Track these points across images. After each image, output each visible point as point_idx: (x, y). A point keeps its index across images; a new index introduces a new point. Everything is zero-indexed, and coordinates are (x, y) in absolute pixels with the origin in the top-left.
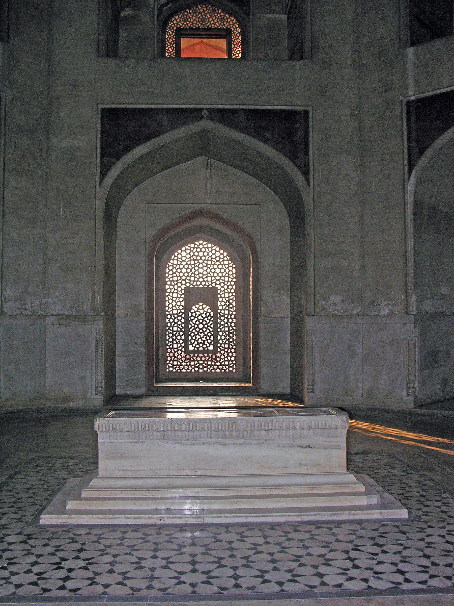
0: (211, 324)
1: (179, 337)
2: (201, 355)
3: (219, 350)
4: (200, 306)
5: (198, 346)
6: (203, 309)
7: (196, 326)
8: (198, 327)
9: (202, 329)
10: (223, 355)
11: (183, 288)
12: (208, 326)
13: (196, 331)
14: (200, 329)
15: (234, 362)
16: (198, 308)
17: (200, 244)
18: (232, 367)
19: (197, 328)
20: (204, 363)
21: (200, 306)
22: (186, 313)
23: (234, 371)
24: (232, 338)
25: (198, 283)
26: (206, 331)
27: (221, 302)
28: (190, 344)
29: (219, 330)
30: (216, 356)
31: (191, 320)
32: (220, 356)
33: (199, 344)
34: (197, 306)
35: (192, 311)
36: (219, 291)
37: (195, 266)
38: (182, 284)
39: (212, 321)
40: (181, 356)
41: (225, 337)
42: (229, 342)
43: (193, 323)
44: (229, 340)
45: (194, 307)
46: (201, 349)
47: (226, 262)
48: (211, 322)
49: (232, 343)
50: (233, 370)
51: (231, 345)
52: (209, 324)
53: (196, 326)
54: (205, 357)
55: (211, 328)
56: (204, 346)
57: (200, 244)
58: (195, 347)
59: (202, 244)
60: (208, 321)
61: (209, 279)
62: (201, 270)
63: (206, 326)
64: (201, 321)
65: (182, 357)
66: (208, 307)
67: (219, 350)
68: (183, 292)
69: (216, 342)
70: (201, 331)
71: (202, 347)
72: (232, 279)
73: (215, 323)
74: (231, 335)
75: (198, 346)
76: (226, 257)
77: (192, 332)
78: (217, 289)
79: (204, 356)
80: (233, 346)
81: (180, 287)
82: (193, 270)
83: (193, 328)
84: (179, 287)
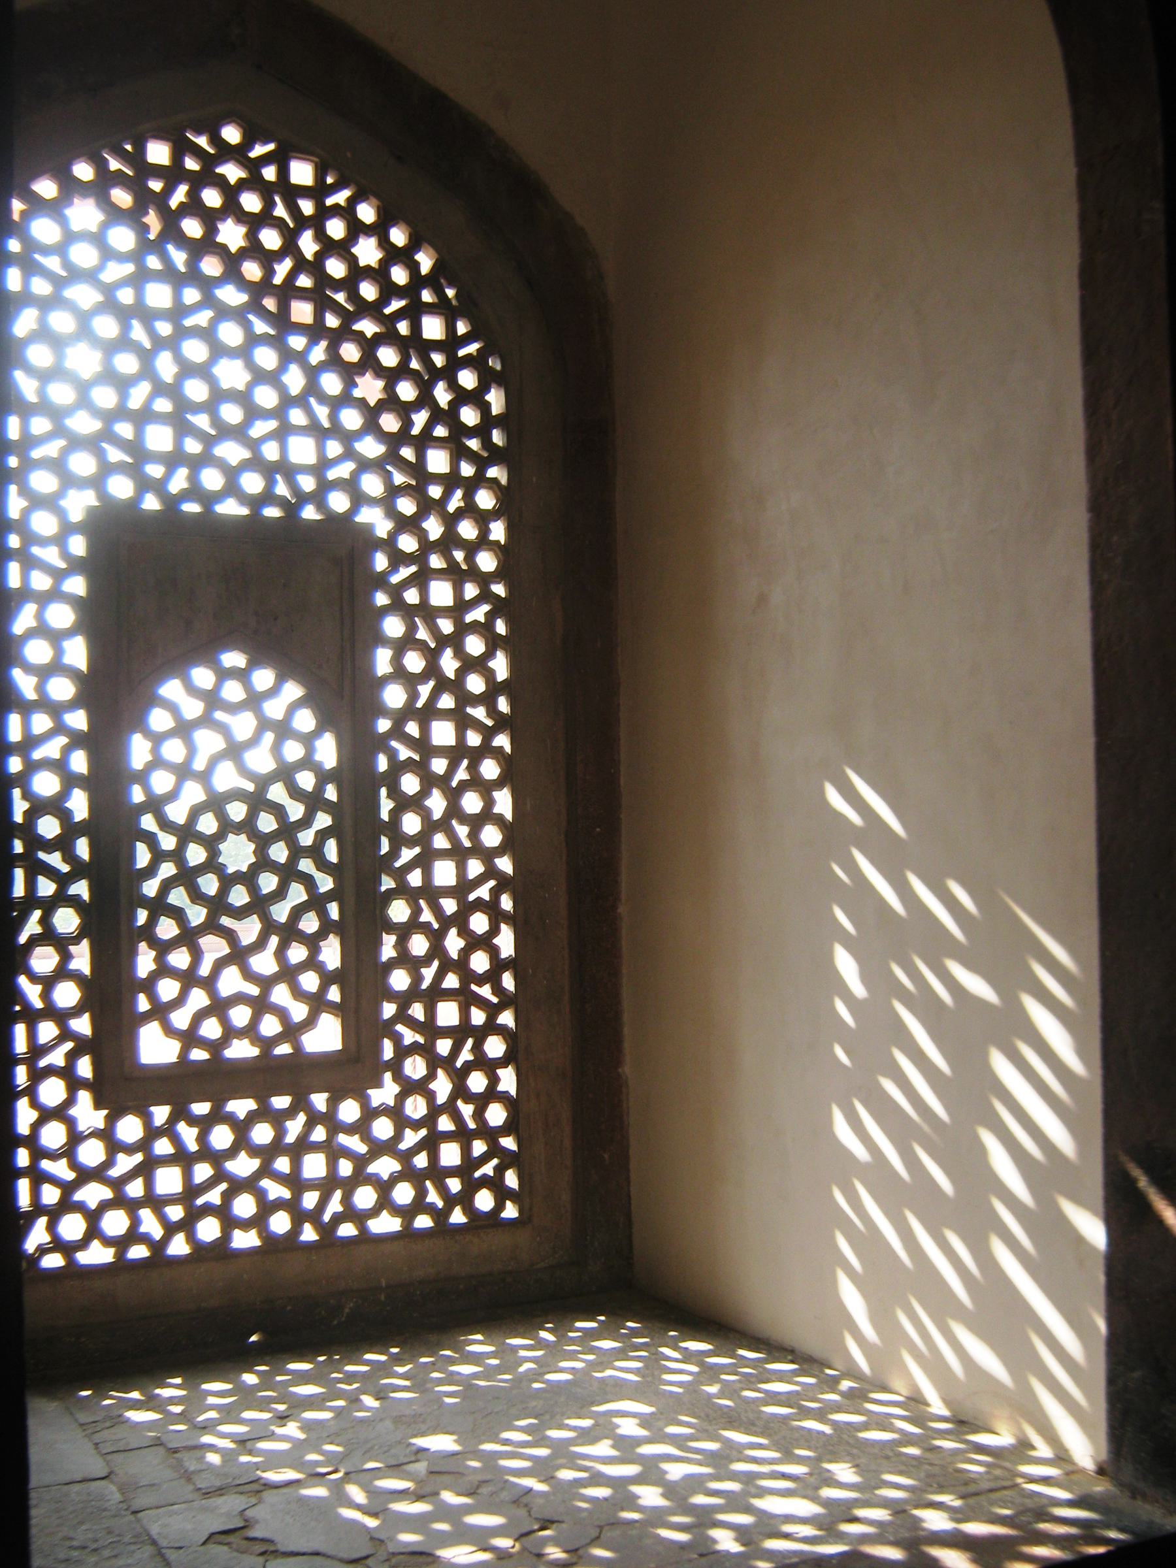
0: (323, 835)
2: (241, 1107)
3: (388, 1051)
4: (223, 674)
5: (211, 1029)
6: (254, 701)
7: (196, 855)
8: (212, 865)
9: (248, 878)
10: (421, 1087)
11: (76, 515)
12: (296, 852)
13: (197, 896)
14: (228, 881)
16: (212, 699)
17: (226, 152)
18: (495, 1184)
19: (202, 869)
21: (223, 674)
23: (510, 1211)
24: (485, 943)
25: (212, 480)
26: (280, 894)
28: (146, 1017)
29: (387, 883)
31: (155, 805)
32: (401, 1098)
33: (219, 1007)
34: (203, 676)
35: (159, 720)
36: (381, 562)
37: (182, 333)
38: (69, 481)
40: (71, 1123)
41: (437, 938)
42: (468, 976)
43: (165, 824)
44: (461, 966)
45: (172, 689)
46: (241, 1050)
47: (433, 328)
48: (323, 820)
49: (485, 991)
50: (499, 1206)
51: (482, 1003)
52: (306, 838)
53: (196, 855)
56: (270, 1026)
57: (226, 152)
58: (190, 1038)
59: (237, 153)
61: (302, 450)
62: (231, 374)
63: (279, 853)
64: (237, 811)
65: (75, 1138)
66: (293, 691)
67: (388, 1051)
68: (78, 546)
69: (360, 985)
70: (239, 896)
72: (482, 464)
74: (479, 923)
76: (433, 281)
77: (159, 907)
78: (367, 542)
79: (263, 1113)
80: (492, 1011)
82: (166, 366)
83: (167, 870)
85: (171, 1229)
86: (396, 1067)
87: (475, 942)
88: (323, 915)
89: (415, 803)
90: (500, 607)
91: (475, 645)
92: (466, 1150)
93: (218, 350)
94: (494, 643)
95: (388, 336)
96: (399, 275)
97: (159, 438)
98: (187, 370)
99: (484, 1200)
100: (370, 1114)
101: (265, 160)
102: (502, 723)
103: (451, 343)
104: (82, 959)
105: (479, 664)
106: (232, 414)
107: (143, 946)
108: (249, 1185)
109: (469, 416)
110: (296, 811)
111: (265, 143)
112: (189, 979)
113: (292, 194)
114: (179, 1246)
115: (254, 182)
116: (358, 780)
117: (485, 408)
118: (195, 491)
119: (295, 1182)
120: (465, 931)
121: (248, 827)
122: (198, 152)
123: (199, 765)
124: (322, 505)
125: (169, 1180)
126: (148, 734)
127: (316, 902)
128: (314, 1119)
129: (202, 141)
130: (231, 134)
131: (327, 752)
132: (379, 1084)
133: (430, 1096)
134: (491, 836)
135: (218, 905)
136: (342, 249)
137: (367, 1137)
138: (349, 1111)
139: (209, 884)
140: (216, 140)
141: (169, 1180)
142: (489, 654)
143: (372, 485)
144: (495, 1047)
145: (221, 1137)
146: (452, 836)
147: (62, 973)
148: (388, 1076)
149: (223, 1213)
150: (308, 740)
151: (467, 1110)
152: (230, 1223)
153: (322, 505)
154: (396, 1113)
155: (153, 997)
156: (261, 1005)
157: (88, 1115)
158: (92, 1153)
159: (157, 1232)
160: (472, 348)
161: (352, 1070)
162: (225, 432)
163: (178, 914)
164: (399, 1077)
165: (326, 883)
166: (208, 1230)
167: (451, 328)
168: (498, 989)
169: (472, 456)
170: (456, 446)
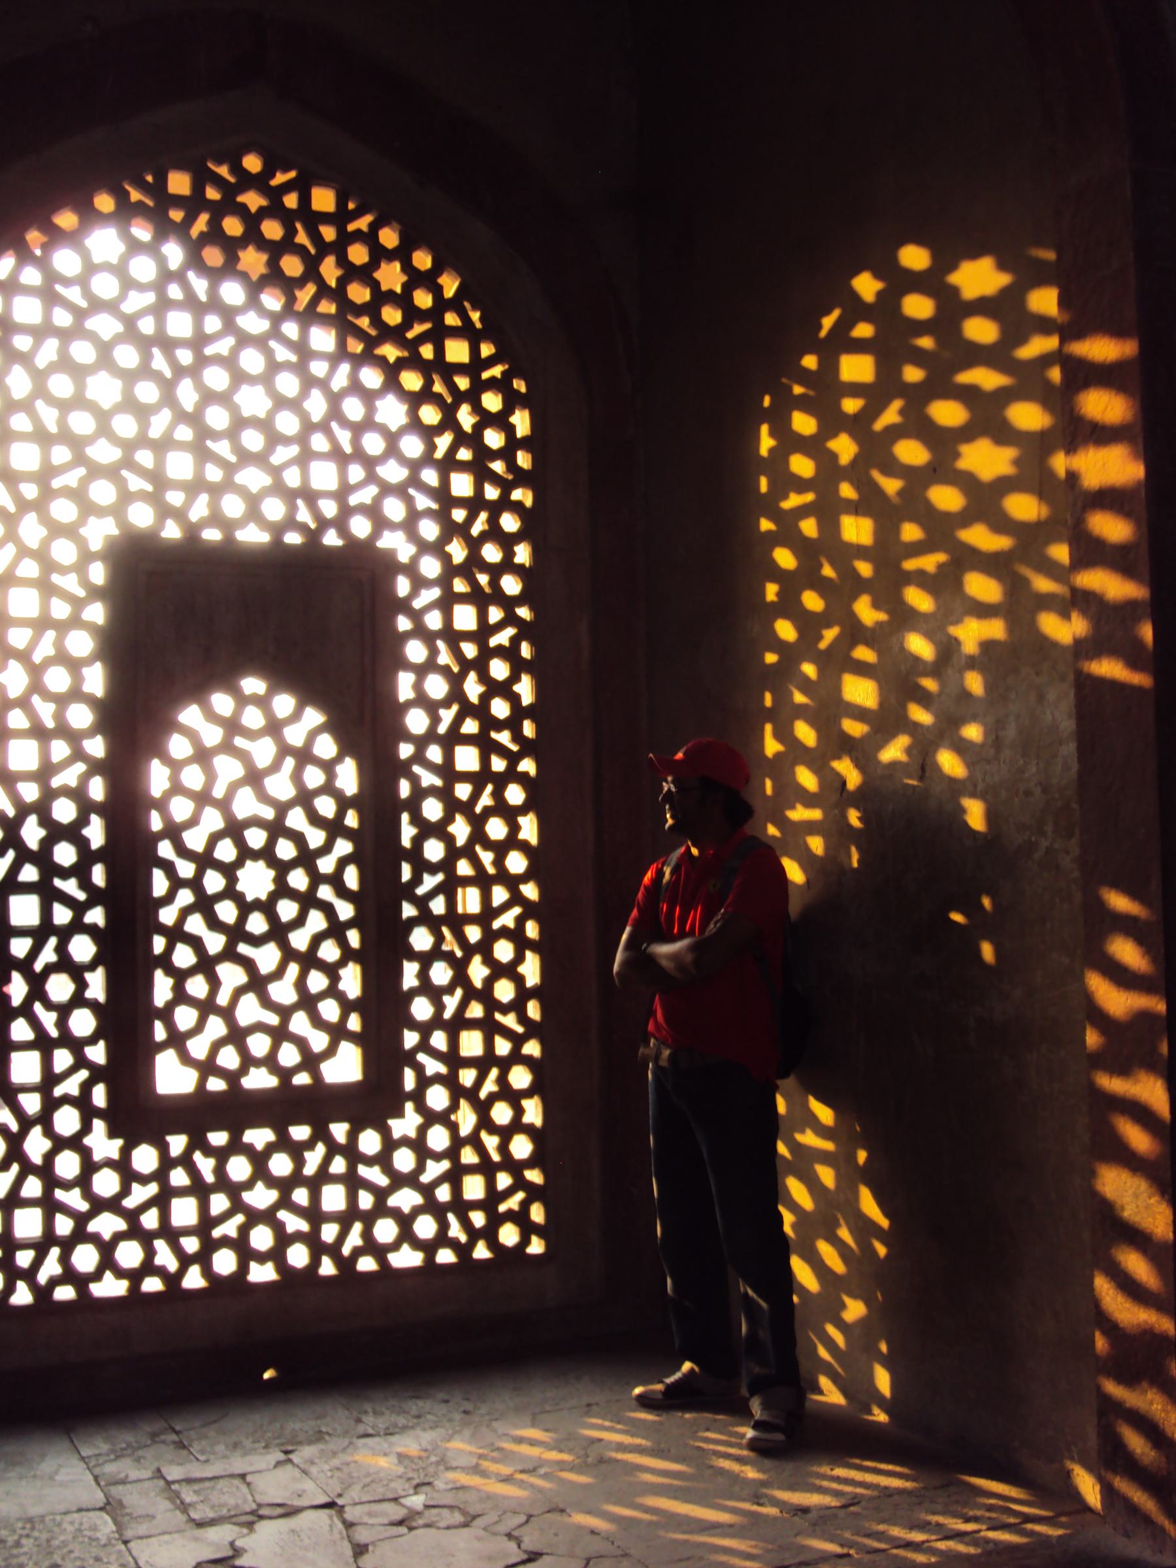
1: (60, 987)
2: (259, 1137)
4: (242, 700)
9: (267, 907)
11: (96, 545)
13: (214, 923)
14: (245, 908)
15: (534, 1176)
16: (232, 726)
17: (247, 181)
18: (520, 1218)
20: (285, 1202)
21: (242, 700)
22: (123, 769)
23: (536, 1247)
25: (233, 506)
27: (422, 671)
30: (385, 1132)
31: (173, 832)
32: (422, 1130)
34: (222, 702)
35: (179, 747)
36: (403, 586)
37: (202, 361)
38: (88, 509)
39: (348, 834)
40: (86, 1154)
41: (460, 968)
42: (492, 1005)
43: (183, 852)
44: (485, 995)
45: (190, 716)
46: (259, 1080)
47: (457, 351)
48: (343, 847)
50: (525, 1241)
51: (507, 1033)
54: (297, 1151)
55: (342, 891)
57: (247, 181)
59: (259, 182)
60: (316, 838)
61: (324, 476)
62: (253, 401)
64: (256, 838)
66: (313, 717)
67: (409, 1080)
68: (98, 574)
69: (382, 1012)
70: (257, 924)
71: (270, 1062)
72: (506, 487)
73: (378, 850)
74: (504, 951)
75: (229, 1058)
76: (455, 304)
77: (176, 934)
78: (388, 566)
81: (70, 531)
84: (57, 530)
85: (185, 1261)
86: (418, 1097)
87: (499, 970)
88: (343, 943)
89: (439, 830)
90: (525, 631)
91: (499, 669)
92: (491, 1184)
93: (239, 378)
94: (518, 667)
95: (413, 361)
96: (423, 299)
97: (180, 466)
98: (209, 397)
99: (509, 1235)
100: (390, 1145)
101: (287, 187)
102: (527, 748)
103: (475, 366)
104: (97, 985)
105: (504, 689)
106: (253, 440)
107: (159, 974)
108: (268, 1217)
109: (494, 439)
110: (316, 838)
111: (286, 170)
112: (207, 1007)
113: (313, 220)
114: (194, 1280)
115: (275, 209)
116: (379, 805)
117: (510, 430)
118: (216, 518)
119: (315, 1215)
120: (489, 960)
121: (267, 854)
122: (219, 182)
123: (218, 792)
124: (343, 531)
125: (184, 1212)
126: (168, 760)
127: (336, 930)
128: (333, 1150)
129: (223, 171)
130: (252, 163)
131: (348, 778)
132: (400, 1114)
133: (453, 1128)
134: (516, 863)
135: (236, 933)
136: (365, 274)
137: (388, 1169)
138: (370, 1142)
139: (227, 912)
140: (237, 169)
141: (184, 1212)
142: (515, 678)
143: (394, 509)
144: (520, 1078)
145: (239, 1168)
146: (476, 862)
147: (78, 1000)
148: (409, 1106)
149: (241, 1245)
150: (328, 767)
151: (491, 1142)
152: (246, 1254)
153: (343, 531)
154: (419, 1146)
155: (170, 1026)
156: (280, 1034)
157: (103, 1144)
158: (106, 1183)
159: (172, 1265)
160: (497, 371)
161: (374, 1100)
162: (246, 458)
163: (196, 943)
164: (422, 1108)
165: (345, 911)
166: (225, 1262)
167: (475, 351)
168: (523, 1019)
169: (495, 479)
170: (479, 470)
